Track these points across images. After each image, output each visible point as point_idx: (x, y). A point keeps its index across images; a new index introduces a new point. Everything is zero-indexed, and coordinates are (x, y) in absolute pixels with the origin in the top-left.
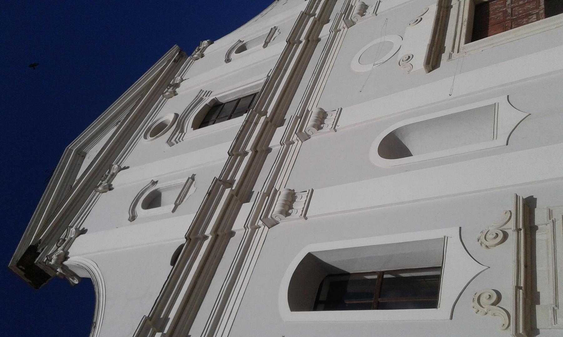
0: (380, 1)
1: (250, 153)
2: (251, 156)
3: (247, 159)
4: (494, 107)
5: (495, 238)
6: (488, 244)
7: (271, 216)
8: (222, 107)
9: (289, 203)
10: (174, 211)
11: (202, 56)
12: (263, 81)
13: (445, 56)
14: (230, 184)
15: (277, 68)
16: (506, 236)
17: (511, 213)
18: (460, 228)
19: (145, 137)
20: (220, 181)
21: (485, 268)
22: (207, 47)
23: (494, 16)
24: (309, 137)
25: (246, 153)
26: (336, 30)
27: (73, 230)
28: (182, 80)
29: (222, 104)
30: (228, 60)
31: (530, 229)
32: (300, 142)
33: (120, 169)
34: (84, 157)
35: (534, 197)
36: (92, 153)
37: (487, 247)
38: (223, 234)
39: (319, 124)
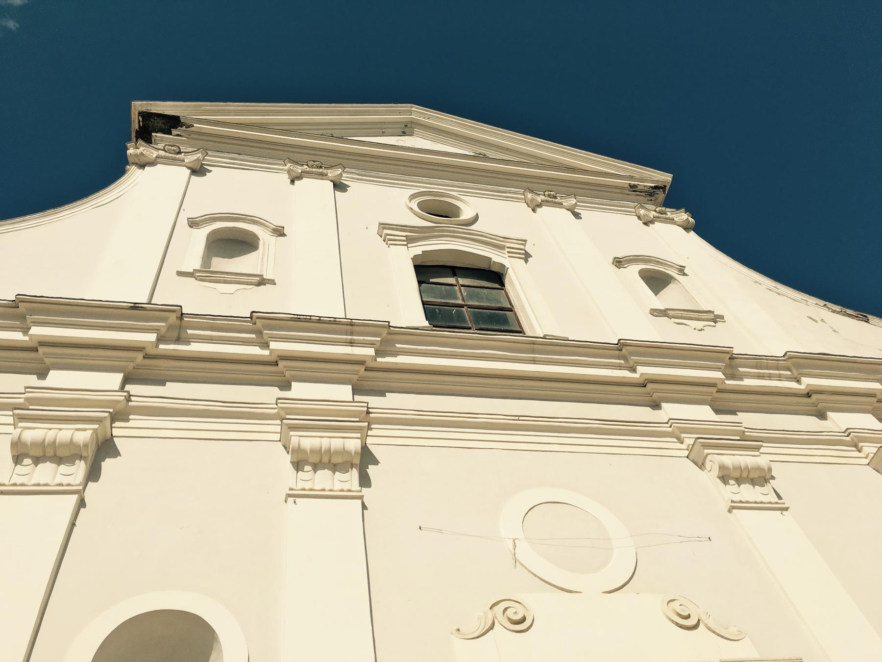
8: (497, 286)
10: (180, 274)
22: (675, 223)
25: (265, 345)
29: (503, 285)
30: (619, 262)
34: (404, 134)
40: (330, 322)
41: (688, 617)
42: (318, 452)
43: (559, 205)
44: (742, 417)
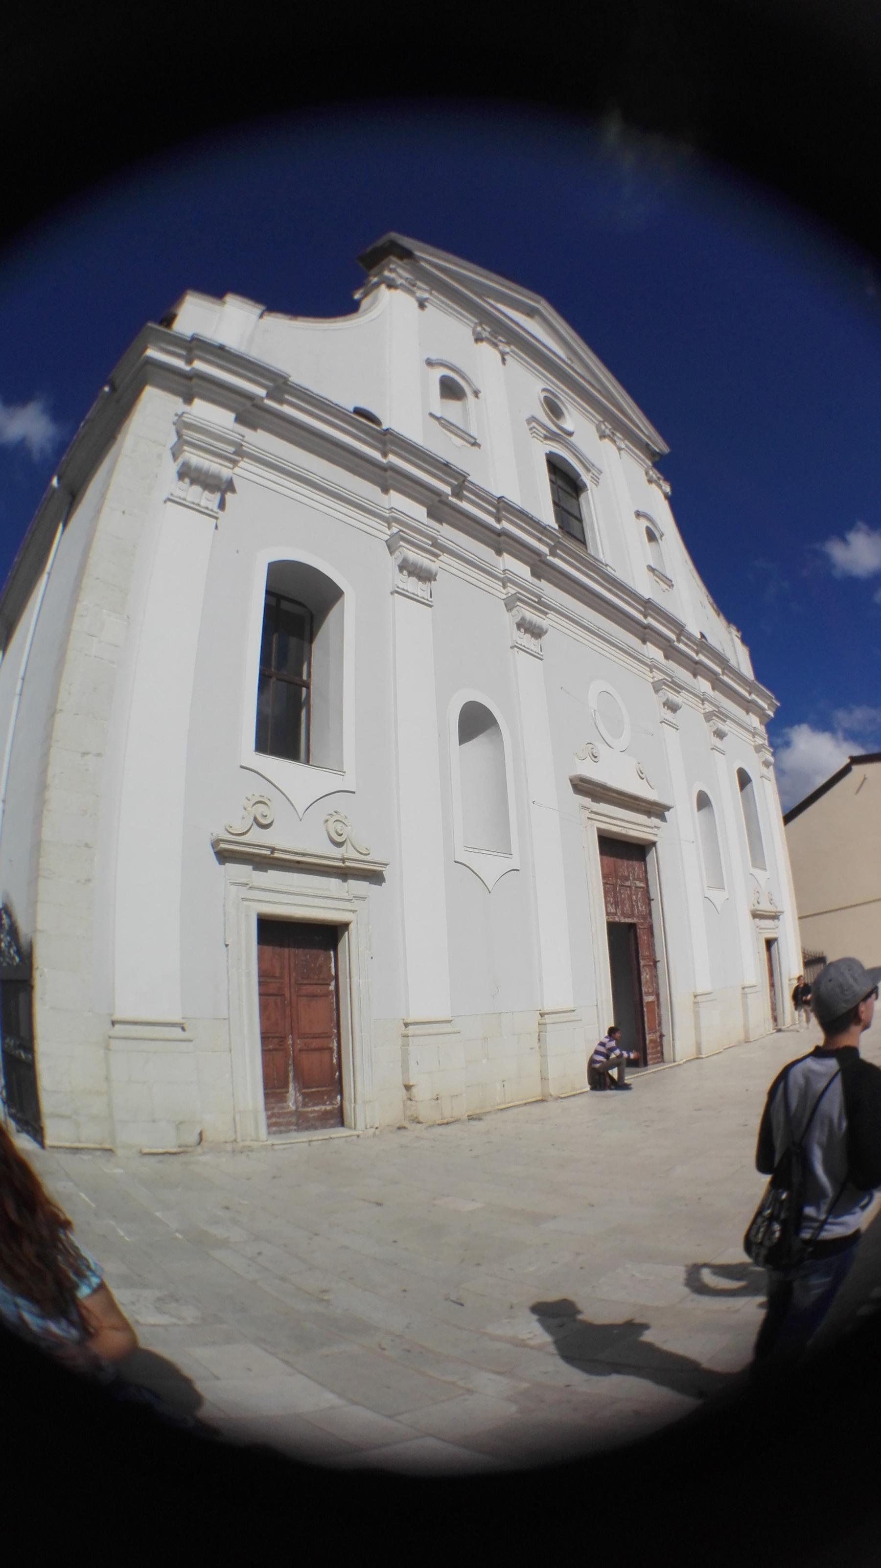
1: (498, 526)
2: (495, 528)
5: (337, 832)
6: (330, 823)
7: (401, 546)
8: (574, 495)
9: (417, 572)
10: (431, 415)
11: (650, 481)
12: (601, 557)
13: (587, 801)
14: (457, 494)
15: (615, 580)
16: (339, 845)
17: (366, 855)
18: (354, 793)
19: (544, 390)
20: (464, 481)
21: (301, 815)
23: (625, 866)
24: (509, 610)
25: (499, 520)
26: (652, 667)
27: (426, 295)
28: (620, 449)
30: (638, 514)
31: (344, 873)
32: (505, 597)
33: (503, 355)
36: (533, 327)
37: (327, 821)
38: (386, 478)
39: (524, 626)
43: (614, 442)
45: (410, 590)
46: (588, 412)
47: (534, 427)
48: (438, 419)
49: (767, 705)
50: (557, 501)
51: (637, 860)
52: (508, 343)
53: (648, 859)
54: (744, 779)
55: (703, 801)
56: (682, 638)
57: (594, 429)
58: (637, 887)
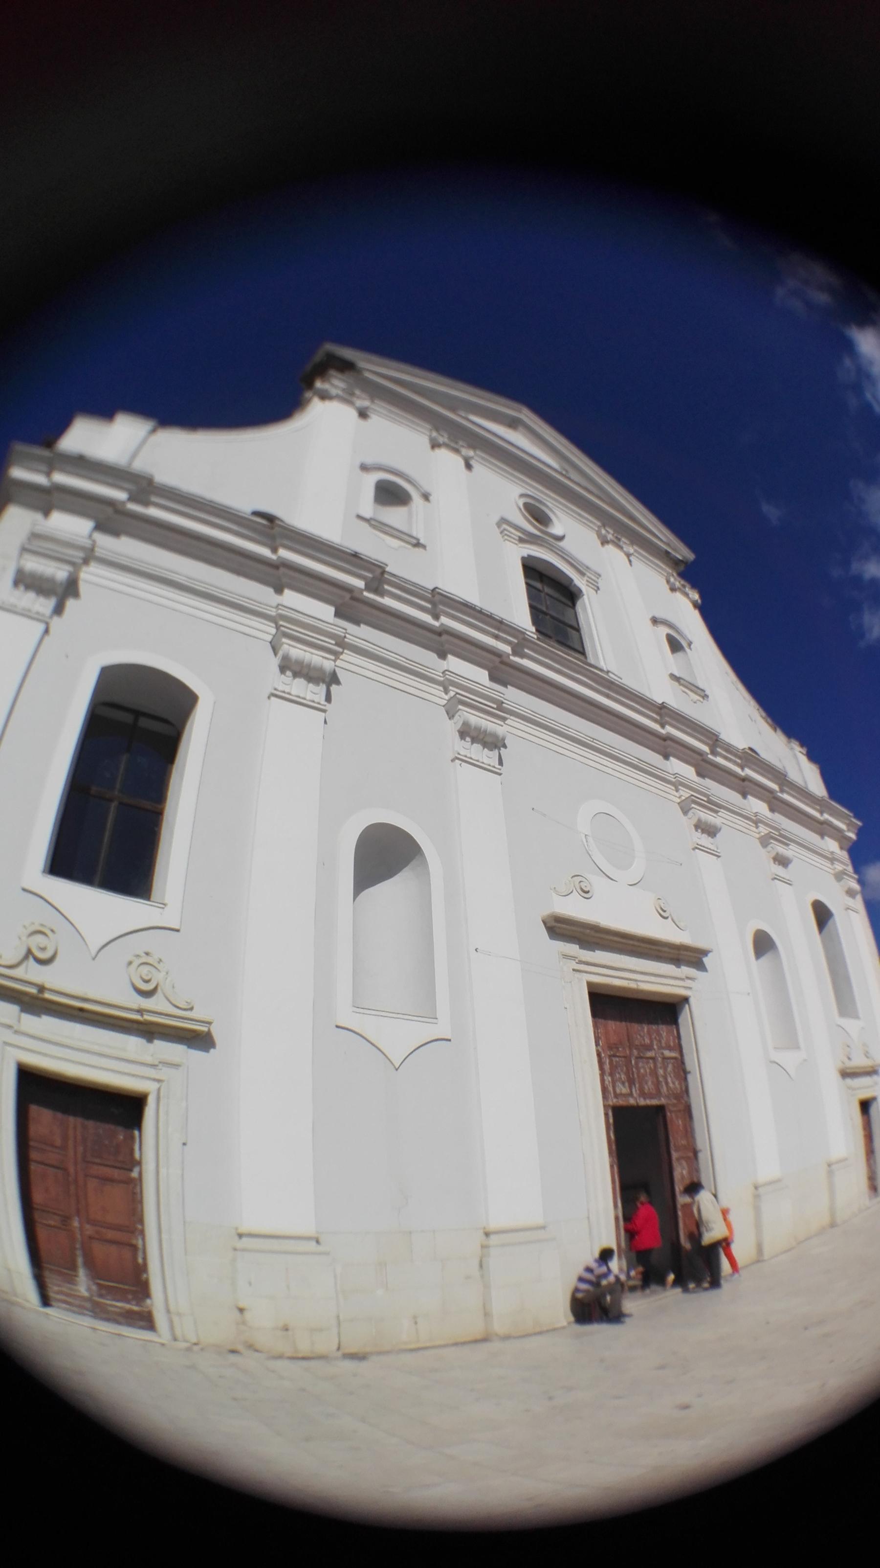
0: (719, 857)
1: (436, 624)
3: (427, 618)
4: (434, 1017)
8: (570, 604)
10: (359, 517)
11: (673, 589)
12: (602, 664)
13: (573, 949)
19: (522, 496)
23: (643, 1032)
25: (436, 617)
28: (628, 555)
29: (574, 605)
30: (655, 621)
31: (149, 1031)
35: (212, 1050)
36: (518, 439)
37: (130, 963)
38: (278, 576)
40: (487, 616)
41: (665, 911)
42: (478, 729)
43: (621, 548)
44: (708, 782)
45: (293, 693)
46: (591, 522)
47: (505, 529)
48: (367, 520)
49: (846, 825)
50: (535, 604)
51: (665, 1022)
52: (473, 447)
53: (681, 1020)
54: (822, 915)
55: (763, 944)
56: (719, 750)
57: (595, 536)
58: (664, 1058)
